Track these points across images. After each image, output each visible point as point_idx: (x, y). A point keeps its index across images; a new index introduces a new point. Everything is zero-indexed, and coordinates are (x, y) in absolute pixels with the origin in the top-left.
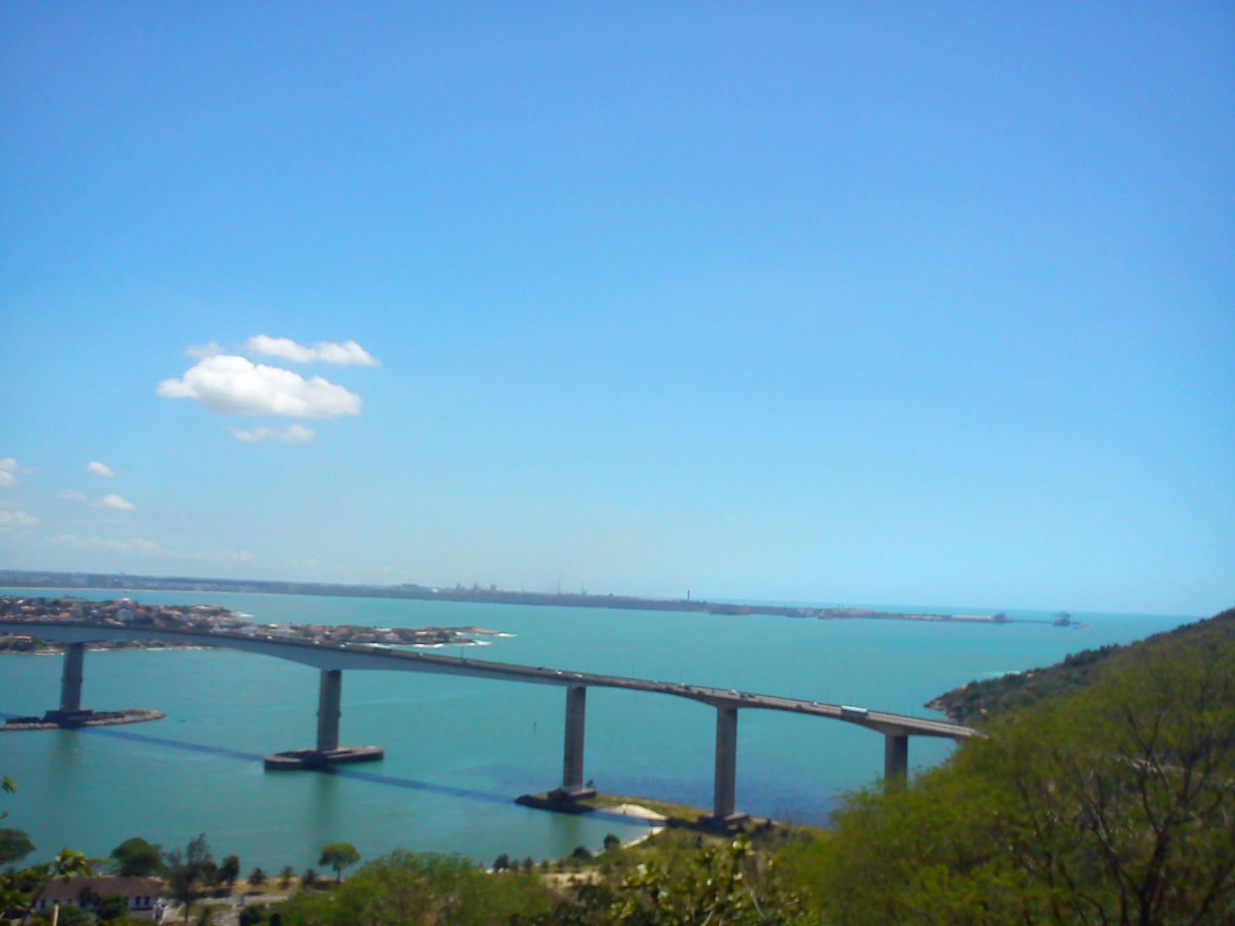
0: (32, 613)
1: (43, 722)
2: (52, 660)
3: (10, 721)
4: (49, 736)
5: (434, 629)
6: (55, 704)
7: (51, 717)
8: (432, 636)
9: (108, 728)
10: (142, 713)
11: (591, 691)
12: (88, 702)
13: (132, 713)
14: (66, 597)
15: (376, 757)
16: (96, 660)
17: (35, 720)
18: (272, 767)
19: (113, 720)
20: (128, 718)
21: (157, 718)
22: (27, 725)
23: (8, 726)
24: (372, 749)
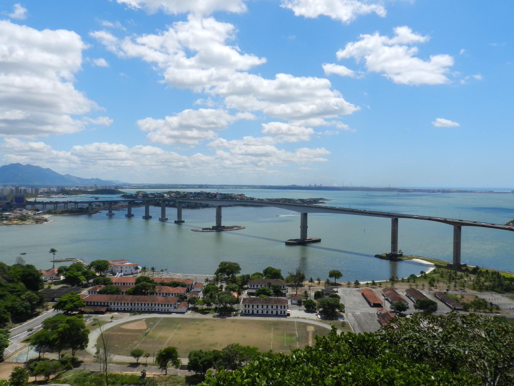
0: (193, 197)
1: (212, 229)
2: (212, 212)
3: (203, 229)
4: (213, 234)
5: (312, 199)
6: (214, 224)
7: (214, 228)
8: (311, 201)
9: (230, 231)
10: (238, 227)
11: (400, 220)
12: (223, 224)
13: (235, 227)
14: (201, 192)
15: (319, 241)
16: (225, 212)
17: (210, 229)
18: (288, 244)
19: (232, 229)
20: (235, 228)
21: (243, 228)
22: (208, 230)
23: (204, 230)
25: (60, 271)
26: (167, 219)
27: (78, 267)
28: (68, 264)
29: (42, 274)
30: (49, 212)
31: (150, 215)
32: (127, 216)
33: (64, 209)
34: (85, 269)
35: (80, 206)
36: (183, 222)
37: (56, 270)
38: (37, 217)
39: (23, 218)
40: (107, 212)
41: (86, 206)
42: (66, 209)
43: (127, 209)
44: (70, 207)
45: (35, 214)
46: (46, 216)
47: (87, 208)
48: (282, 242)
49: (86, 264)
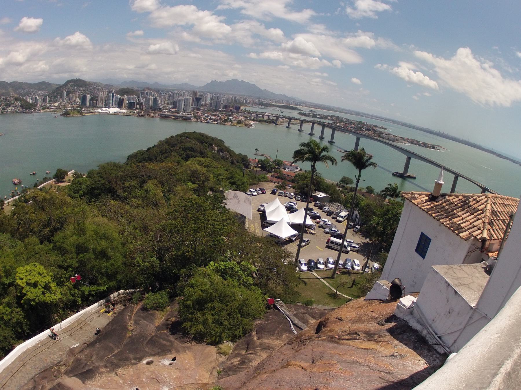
18: (394, 175)
24: (414, 176)
25: (259, 161)
26: (324, 138)
27: (267, 160)
28: (263, 158)
29: (251, 162)
30: (253, 120)
31: (314, 133)
32: (299, 130)
33: (261, 119)
34: (271, 163)
35: (272, 118)
36: (334, 143)
37: (257, 161)
38: (247, 122)
39: (240, 122)
40: (287, 125)
41: (274, 118)
42: (263, 119)
43: (300, 125)
44: (266, 118)
45: (245, 120)
46: (252, 123)
47: (275, 120)
48: (390, 172)
49: (272, 160)
